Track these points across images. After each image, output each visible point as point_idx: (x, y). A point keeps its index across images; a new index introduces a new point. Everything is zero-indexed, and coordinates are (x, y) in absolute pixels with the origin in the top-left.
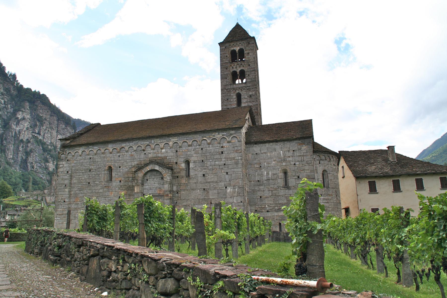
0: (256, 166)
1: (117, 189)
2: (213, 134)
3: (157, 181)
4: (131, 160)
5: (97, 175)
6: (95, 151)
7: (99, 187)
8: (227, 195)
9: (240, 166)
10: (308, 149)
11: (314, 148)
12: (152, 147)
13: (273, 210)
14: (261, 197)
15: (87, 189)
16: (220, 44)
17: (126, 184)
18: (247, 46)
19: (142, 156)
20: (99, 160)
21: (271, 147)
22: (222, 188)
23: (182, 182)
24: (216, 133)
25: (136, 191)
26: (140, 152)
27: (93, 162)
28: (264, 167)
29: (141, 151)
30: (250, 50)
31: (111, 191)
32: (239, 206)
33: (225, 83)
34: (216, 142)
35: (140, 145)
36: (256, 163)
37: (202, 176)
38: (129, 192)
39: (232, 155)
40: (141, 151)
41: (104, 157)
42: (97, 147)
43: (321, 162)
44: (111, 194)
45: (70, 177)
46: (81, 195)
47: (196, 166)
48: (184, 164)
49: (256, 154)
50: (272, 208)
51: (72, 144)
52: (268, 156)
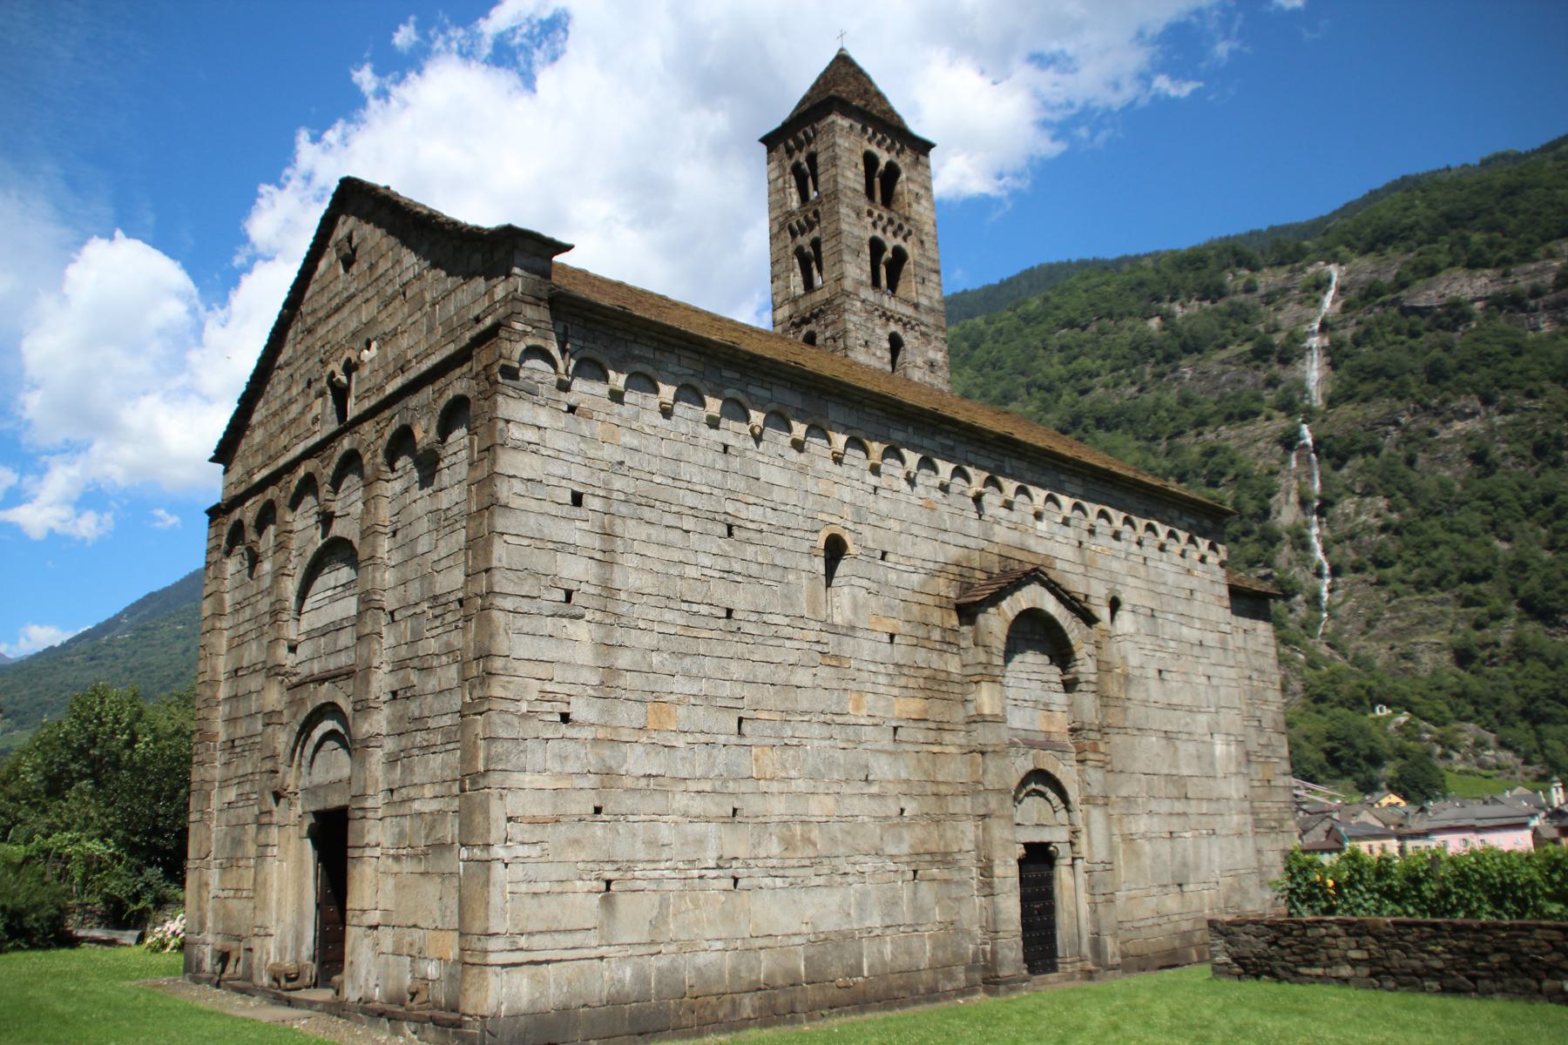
15: (719, 650)
17: (921, 656)
38: (937, 710)
41: (802, 470)
44: (858, 707)
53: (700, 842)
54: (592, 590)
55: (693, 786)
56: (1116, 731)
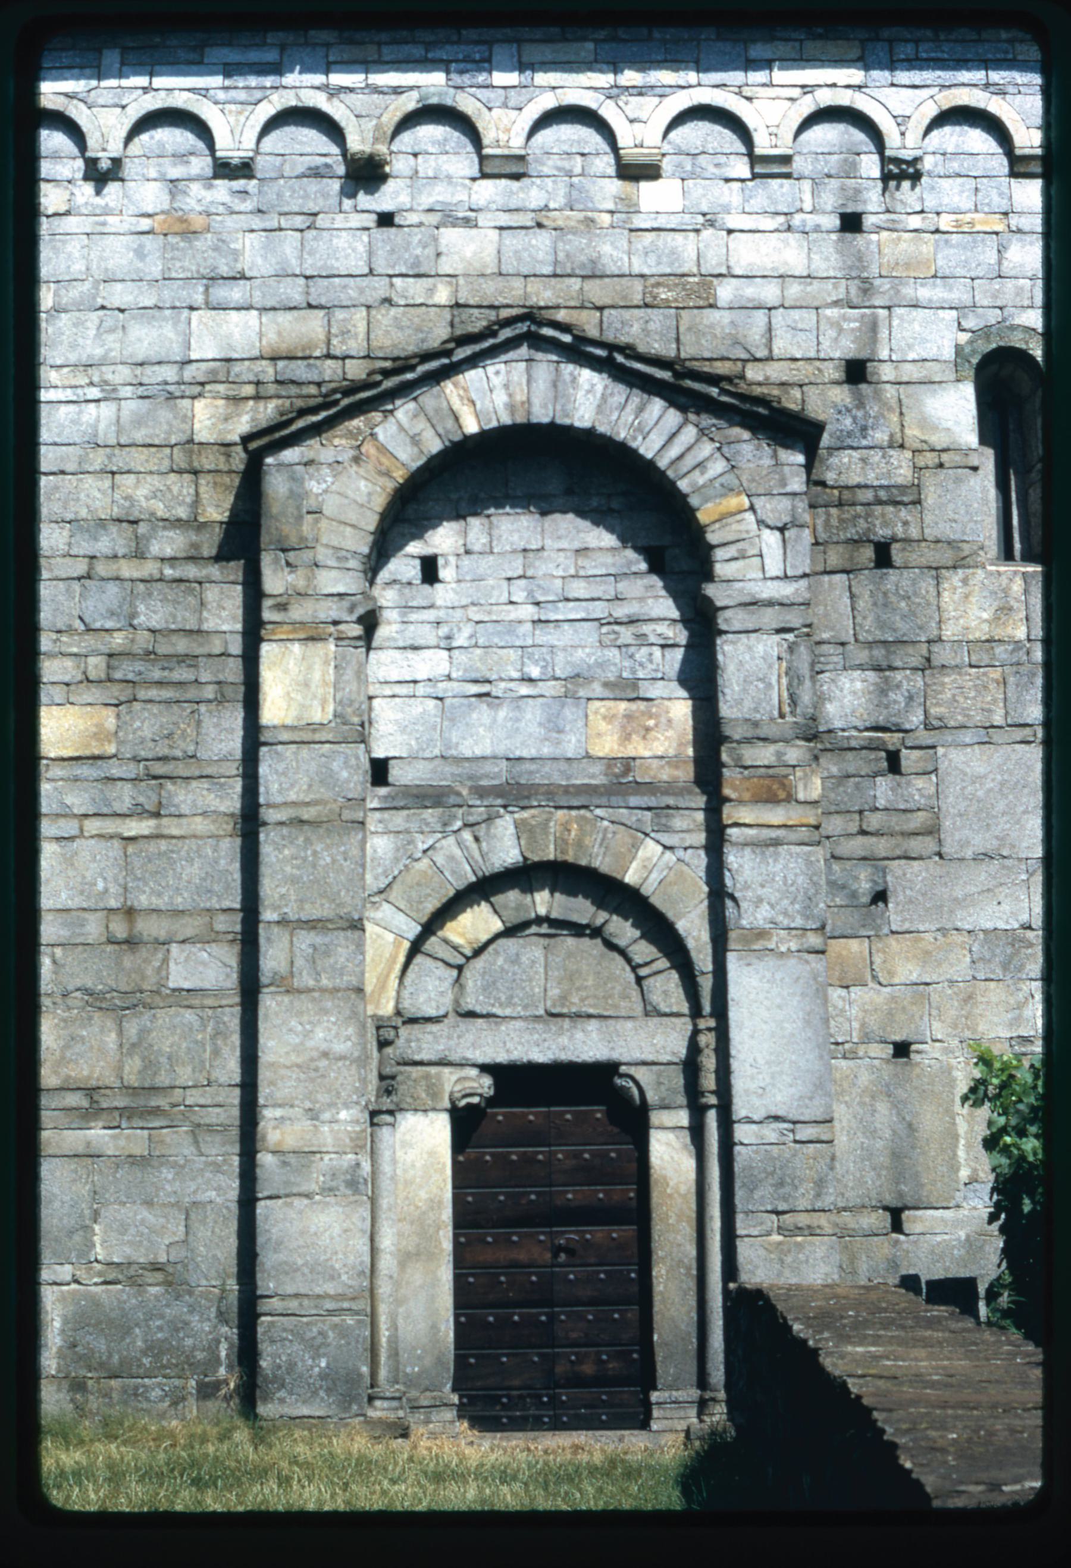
3: (579, 589)
4: (168, 294)
48: (968, 390)
56: (968, 737)
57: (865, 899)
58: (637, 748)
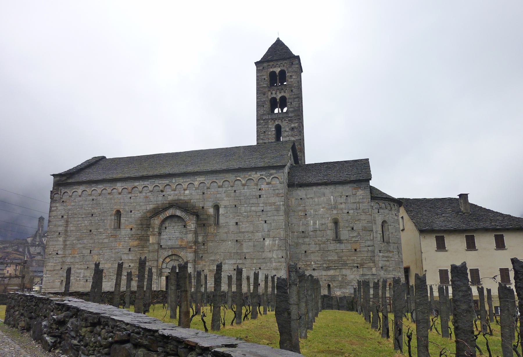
0: (300, 213)
1: (126, 238)
2: (249, 173)
3: (178, 229)
5: (101, 221)
6: (99, 191)
7: (104, 236)
8: (265, 248)
9: (282, 213)
10: (365, 194)
11: (371, 194)
12: (172, 187)
13: (321, 268)
14: (305, 252)
16: (257, 64)
18: (290, 67)
19: (160, 198)
20: (105, 202)
21: (319, 191)
22: (259, 240)
23: (210, 232)
24: (253, 172)
25: (151, 242)
26: (158, 193)
27: (97, 204)
28: (311, 216)
29: (158, 191)
30: (293, 72)
31: (119, 241)
32: (279, 262)
33: (262, 112)
34: (252, 184)
35: (158, 185)
36: (300, 210)
37: (235, 224)
39: (272, 200)
40: (158, 191)
41: (111, 199)
42: (102, 186)
43: (381, 211)
44: (119, 245)
45: (65, 223)
46: (79, 246)
47: (227, 212)
48: (213, 209)
49: (301, 199)
50: (319, 265)
51: (70, 181)
52: (315, 201)
53: (80, 273)
54: (63, 232)
55: (80, 263)
57: (201, 257)
58: (182, 244)
